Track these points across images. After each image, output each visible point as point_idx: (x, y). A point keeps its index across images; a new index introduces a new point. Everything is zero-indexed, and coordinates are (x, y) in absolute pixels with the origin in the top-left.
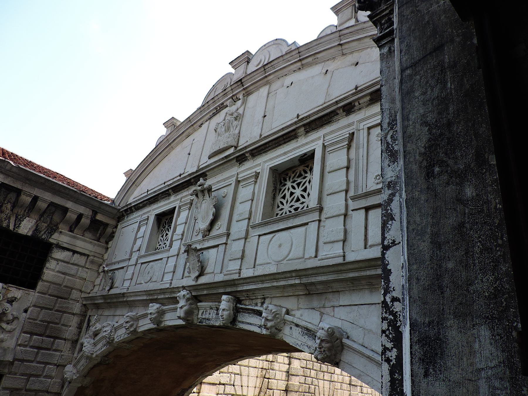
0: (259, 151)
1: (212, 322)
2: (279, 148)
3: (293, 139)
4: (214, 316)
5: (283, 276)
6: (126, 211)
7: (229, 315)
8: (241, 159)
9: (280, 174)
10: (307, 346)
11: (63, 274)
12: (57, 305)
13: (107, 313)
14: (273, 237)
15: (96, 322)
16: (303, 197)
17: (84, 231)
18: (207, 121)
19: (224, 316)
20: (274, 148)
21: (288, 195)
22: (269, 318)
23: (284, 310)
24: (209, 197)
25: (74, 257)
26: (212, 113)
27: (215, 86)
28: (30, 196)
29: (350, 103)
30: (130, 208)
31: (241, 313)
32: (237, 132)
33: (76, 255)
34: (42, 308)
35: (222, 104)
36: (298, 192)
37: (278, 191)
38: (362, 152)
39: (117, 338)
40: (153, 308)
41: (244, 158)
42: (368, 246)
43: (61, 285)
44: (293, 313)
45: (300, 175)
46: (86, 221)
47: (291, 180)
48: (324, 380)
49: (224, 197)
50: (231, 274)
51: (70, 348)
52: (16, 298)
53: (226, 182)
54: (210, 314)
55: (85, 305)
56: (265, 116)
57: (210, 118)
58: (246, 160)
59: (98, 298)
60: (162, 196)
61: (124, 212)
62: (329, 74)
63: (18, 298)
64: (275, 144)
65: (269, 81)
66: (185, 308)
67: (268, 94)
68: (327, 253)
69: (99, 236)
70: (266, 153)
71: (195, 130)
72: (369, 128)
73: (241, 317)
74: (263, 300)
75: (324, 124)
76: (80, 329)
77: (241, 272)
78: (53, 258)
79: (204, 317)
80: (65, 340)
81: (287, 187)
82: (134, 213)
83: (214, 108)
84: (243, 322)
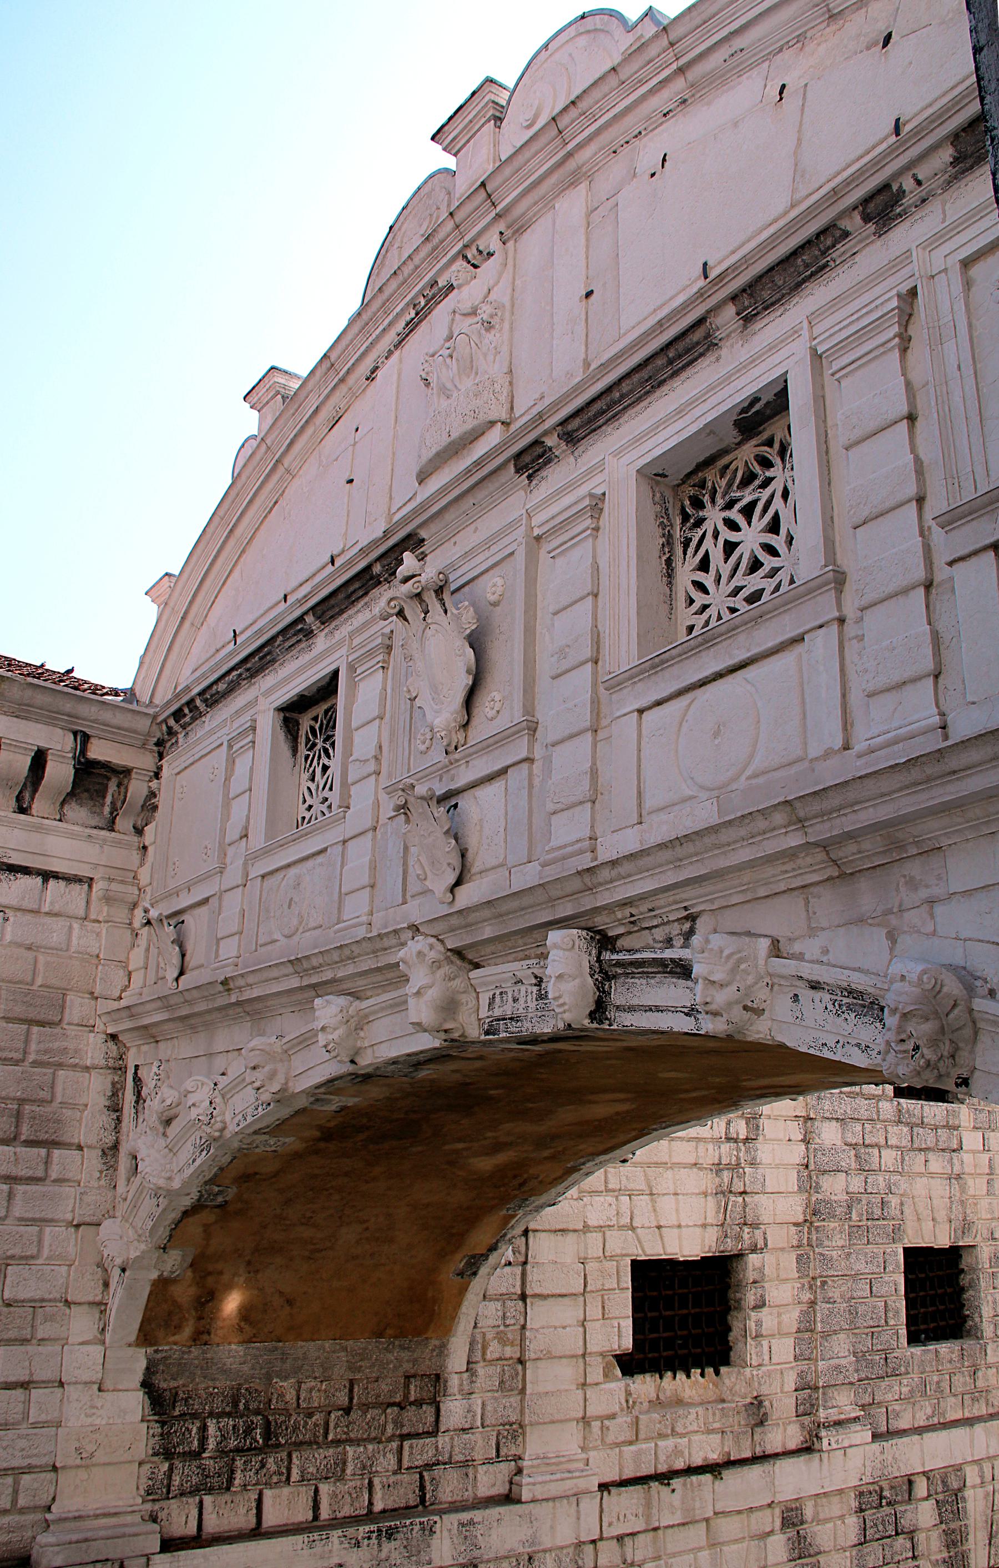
0: (590, 421)
1: (529, 1025)
2: (658, 393)
3: (702, 355)
4: (532, 1005)
6: (178, 715)
10: (858, 1045)
12: (33, 1047)
15: (159, 1084)
17: (63, 804)
18: (390, 353)
20: (640, 400)
21: (717, 555)
23: (764, 944)
24: (446, 612)
25: (49, 891)
26: (403, 324)
29: (886, 187)
31: (622, 979)
33: (52, 882)
37: (679, 550)
39: (236, 1120)
41: (540, 456)
44: (797, 947)
45: (749, 478)
47: (720, 502)
49: (495, 604)
50: (564, 858)
51: (101, 1172)
53: (494, 549)
54: (515, 1000)
55: (114, 1037)
56: (589, 294)
57: (400, 343)
58: (549, 461)
59: (149, 1007)
60: (284, 641)
61: (172, 722)
65: (584, 170)
66: (432, 994)
69: (111, 813)
70: (616, 424)
71: (355, 396)
72: (966, 264)
73: (619, 994)
74: (687, 926)
75: (804, 281)
77: (599, 847)
79: (497, 1012)
81: (708, 526)
82: (203, 719)
83: (407, 305)
84: (631, 1009)
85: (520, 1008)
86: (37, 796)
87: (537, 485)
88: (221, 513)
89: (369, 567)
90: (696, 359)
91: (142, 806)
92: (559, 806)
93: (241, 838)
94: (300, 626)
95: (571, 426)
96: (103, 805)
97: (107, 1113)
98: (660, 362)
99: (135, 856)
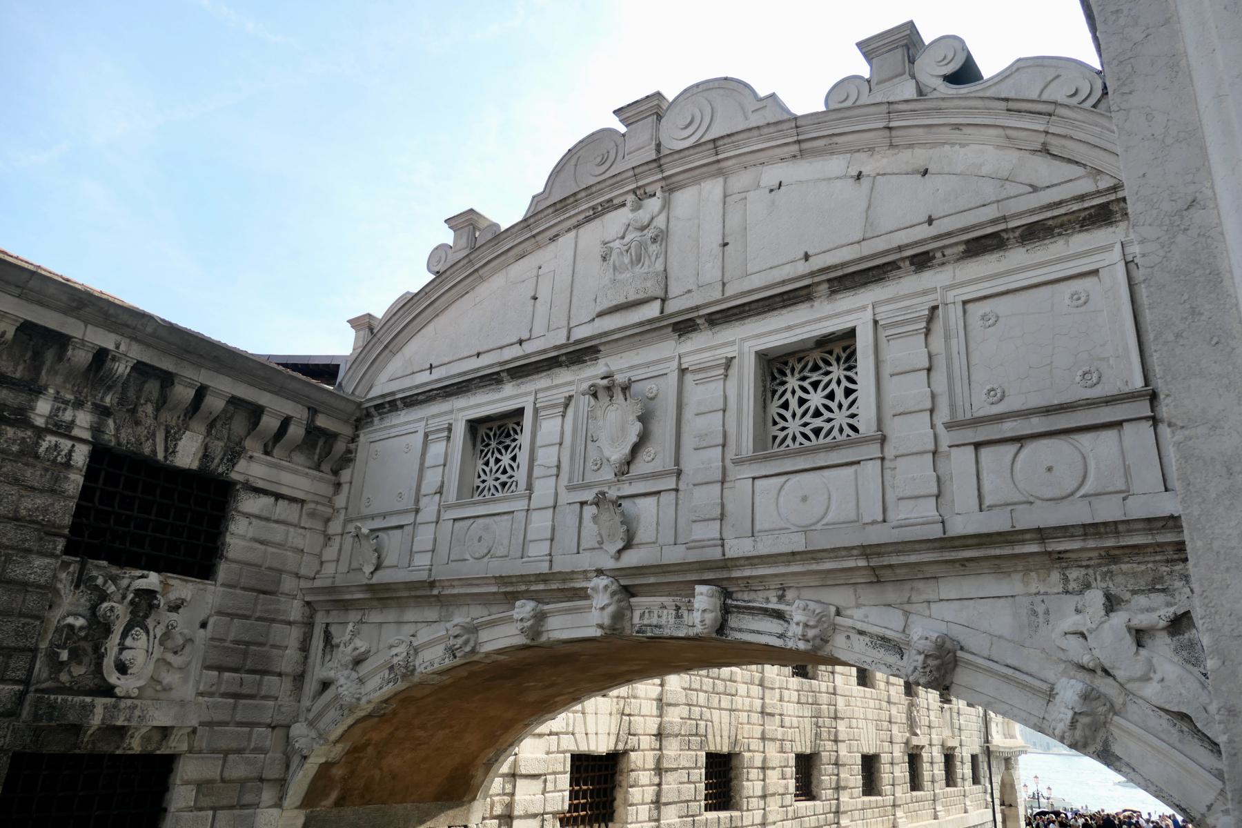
2: (771, 314)
3: (803, 302)
4: (672, 621)
5: (832, 555)
6: (377, 407)
7: (716, 619)
8: (684, 327)
9: (769, 361)
10: (885, 664)
11: (262, 543)
12: (259, 607)
13: (375, 617)
14: (786, 482)
18: (569, 230)
20: (758, 314)
21: (793, 403)
22: (811, 623)
23: (833, 609)
24: (626, 399)
25: (278, 508)
28: (190, 385)
29: (927, 253)
30: (389, 402)
31: (735, 614)
32: (659, 266)
33: (280, 502)
34: (232, 616)
35: (610, 200)
36: (816, 399)
37: (769, 395)
38: (957, 344)
39: (424, 665)
40: (524, 609)
41: (690, 327)
42: (984, 507)
43: (260, 566)
44: (849, 612)
45: (816, 368)
46: (296, 432)
47: (797, 376)
48: (720, 709)
49: (652, 399)
50: (703, 547)
51: (291, 691)
52: (183, 601)
53: (651, 369)
54: (659, 617)
55: (308, 603)
56: (725, 245)
57: (578, 226)
58: (695, 330)
59: (353, 589)
61: (372, 410)
62: (865, 182)
63: (188, 599)
64: (763, 307)
66: (611, 609)
67: (725, 196)
68: (909, 516)
69: (319, 459)
72: (965, 303)
73: (733, 621)
74: (780, 593)
75: (869, 282)
76: (304, 651)
78: (239, 512)
79: (646, 622)
80: (280, 675)
81: (789, 386)
82: (399, 412)
83: (590, 208)
84: (740, 630)
85: (663, 621)
86: (278, 445)
87: (684, 341)
88: (427, 290)
89: (558, 356)
90: (798, 303)
91: (340, 458)
92: (699, 519)
93: (436, 493)
94: (495, 377)
95: (714, 317)
96: (314, 454)
97: (299, 652)
98: (777, 299)
99: (329, 490)
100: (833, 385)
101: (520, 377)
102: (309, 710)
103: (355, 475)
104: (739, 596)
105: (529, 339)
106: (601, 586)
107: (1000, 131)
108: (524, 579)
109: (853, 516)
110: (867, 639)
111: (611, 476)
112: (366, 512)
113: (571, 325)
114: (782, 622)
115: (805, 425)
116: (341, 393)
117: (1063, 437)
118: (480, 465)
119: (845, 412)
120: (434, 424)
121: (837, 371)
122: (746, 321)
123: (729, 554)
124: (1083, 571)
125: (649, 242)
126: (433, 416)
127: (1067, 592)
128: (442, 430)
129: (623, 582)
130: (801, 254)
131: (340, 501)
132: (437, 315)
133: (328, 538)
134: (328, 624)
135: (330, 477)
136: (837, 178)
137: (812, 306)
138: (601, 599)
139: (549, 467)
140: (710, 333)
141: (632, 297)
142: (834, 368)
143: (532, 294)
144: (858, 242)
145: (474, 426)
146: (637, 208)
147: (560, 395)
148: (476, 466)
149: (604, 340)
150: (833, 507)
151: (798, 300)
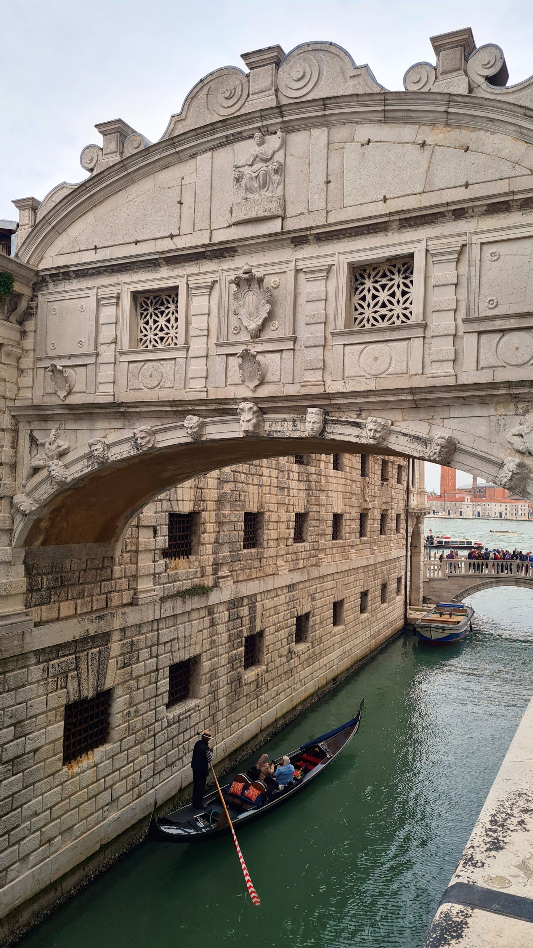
2: (359, 237)
4: (290, 428)
9: (354, 268)
13: (71, 426)
16: (391, 303)
18: (206, 151)
19: (315, 429)
20: (351, 236)
21: (369, 297)
22: (379, 430)
23: (390, 422)
26: (218, 142)
27: (206, 82)
29: (464, 209)
32: (279, 192)
35: (241, 133)
36: (383, 296)
37: (353, 291)
38: (475, 270)
40: (192, 421)
42: (479, 368)
45: (384, 276)
49: (275, 288)
53: (275, 267)
55: (13, 416)
56: (328, 182)
57: (213, 148)
58: (306, 243)
61: (48, 278)
62: (428, 150)
66: (254, 421)
67: (329, 144)
72: (482, 244)
73: (330, 428)
79: (273, 429)
81: (366, 286)
82: (71, 281)
84: (333, 433)
100: (395, 288)
101: (174, 263)
102: (24, 486)
103: (39, 326)
104: (334, 414)
105: (179, 235)
106: (247, 408)
107: (518, 129)
108: (190, 402)
109: (404, 370)
110: (408, 438)
111: (248, 338)
112: (51, 353)
113: (212, 229)
114: (359, 429)
115: (376, 312)
116: (18, 261)
117: (526, 330)
118: (141, 324)
119: (401, 306)
120: (104, 292)
121: (398, 279)
122: (342, 241)
123: (329, 390)
124: (526, 404)
125: (272, 172)
126: (103, 287)
127: (517, 414)
128: (112, 298)
129: (260, 406)
130: (382, 198)
131: (29, 343)
132: (95, 206)
133: (21, 371)
134: (31, 431)
135: (17, 326)
136: (409, 143)
137: (387, 235)
138: (246, 416)
139: (201, 330)
140: (317, 246)
141: (261, 214)
142: (396, 277)
143: (179, 200)
144: (420, 194)
145: (135, 295)
146: (261, 143)
147: (208, 280)
148: (138, 324)
149: (240, 244)
150: (393, 364)
151: (379, 230)
